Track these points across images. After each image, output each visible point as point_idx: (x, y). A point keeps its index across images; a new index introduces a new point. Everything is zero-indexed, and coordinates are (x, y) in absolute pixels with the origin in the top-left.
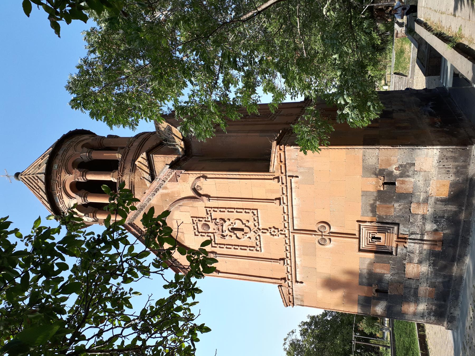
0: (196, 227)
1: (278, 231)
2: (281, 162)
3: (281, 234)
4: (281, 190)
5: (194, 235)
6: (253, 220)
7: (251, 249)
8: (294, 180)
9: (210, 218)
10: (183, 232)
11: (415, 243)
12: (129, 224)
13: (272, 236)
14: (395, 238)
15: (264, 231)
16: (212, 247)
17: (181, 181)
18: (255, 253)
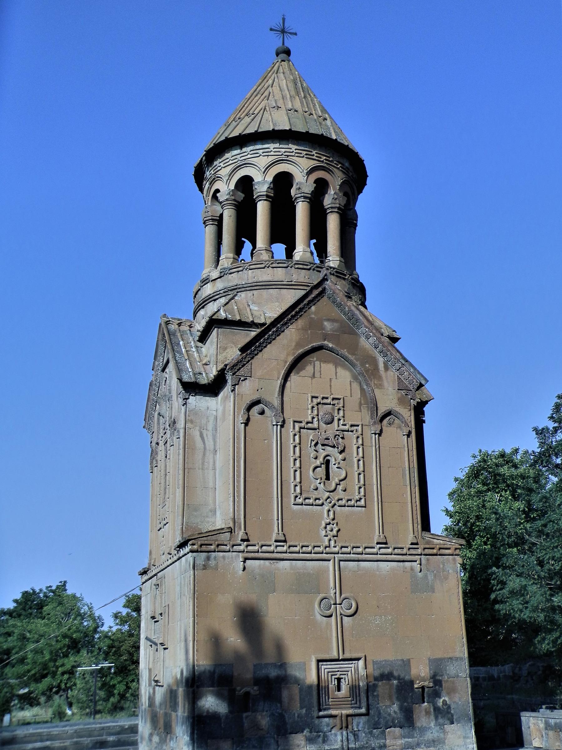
0: (325, 401)
1: (334, 536)
2: (440, 549)
3: (330, 540)
4: (400, 546)
5: (314, 395)
6: (346, 498)
7: (298, 489)
8: (416, 565)
9: (346, 428)
10: (314, 376)
11: (342, 741)
12: (324, 289)
13: (324, 525)
14: (344, 712)
15: (331, 513)
16: (294, 422)
17: (400, 395)
18: (289, 493)
